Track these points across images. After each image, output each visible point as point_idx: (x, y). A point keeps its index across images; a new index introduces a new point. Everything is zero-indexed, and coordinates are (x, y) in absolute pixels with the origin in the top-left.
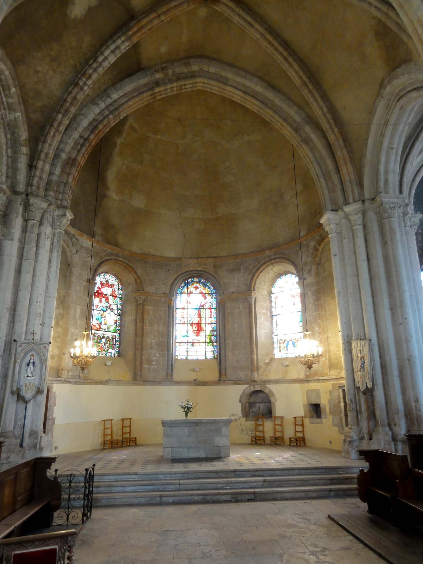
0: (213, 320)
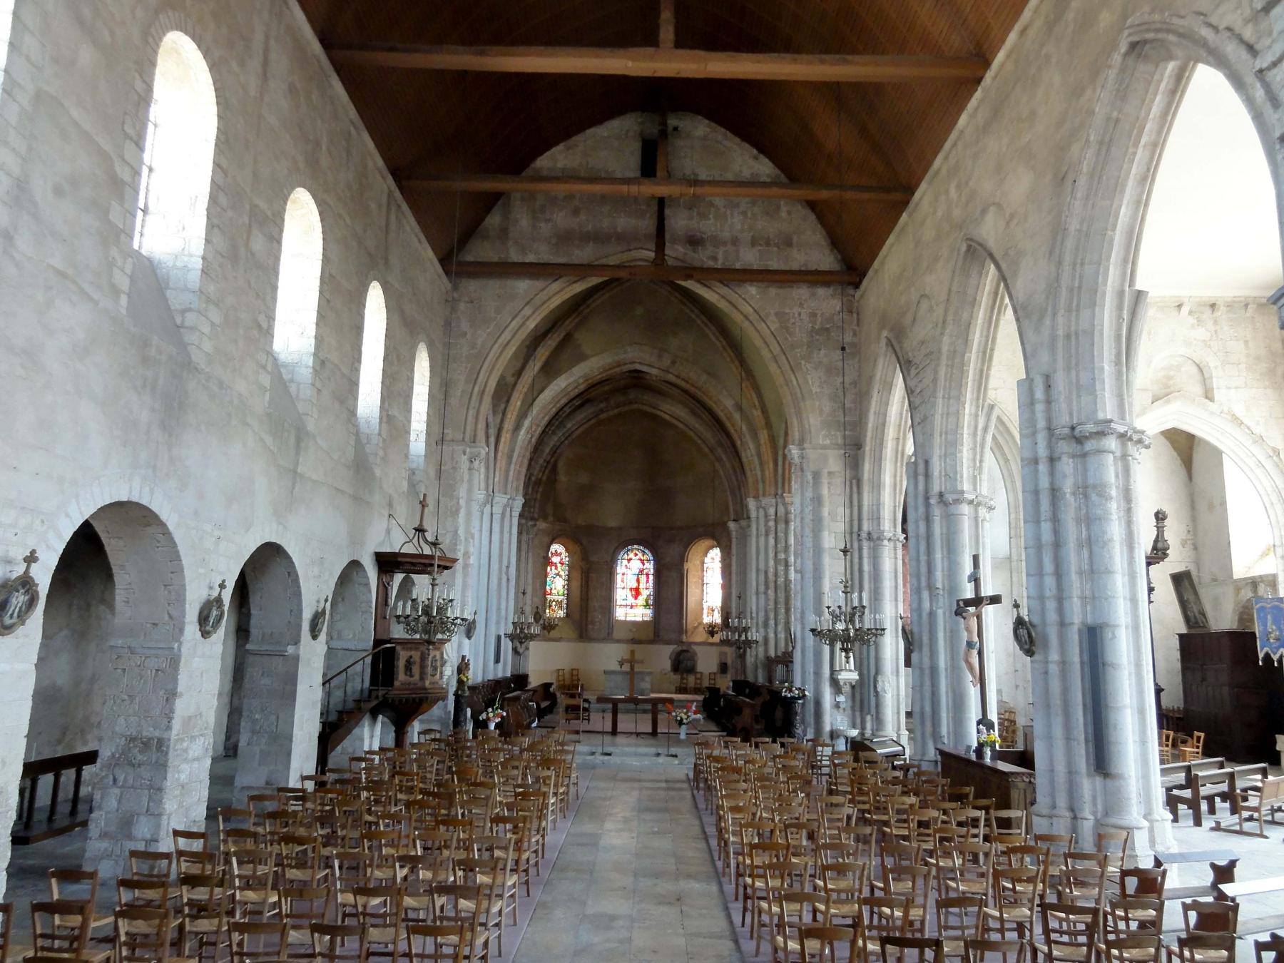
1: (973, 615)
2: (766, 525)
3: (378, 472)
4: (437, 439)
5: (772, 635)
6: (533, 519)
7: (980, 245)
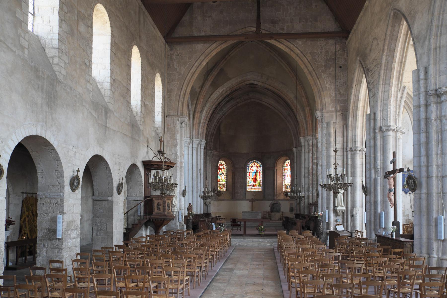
0: (261, 176)
1: (392, 177)
2: (308, 148)
3: (141, 128)
4: (166, 115)
5: (311, 195)
6: (210, 150)
7: (399, 11)
